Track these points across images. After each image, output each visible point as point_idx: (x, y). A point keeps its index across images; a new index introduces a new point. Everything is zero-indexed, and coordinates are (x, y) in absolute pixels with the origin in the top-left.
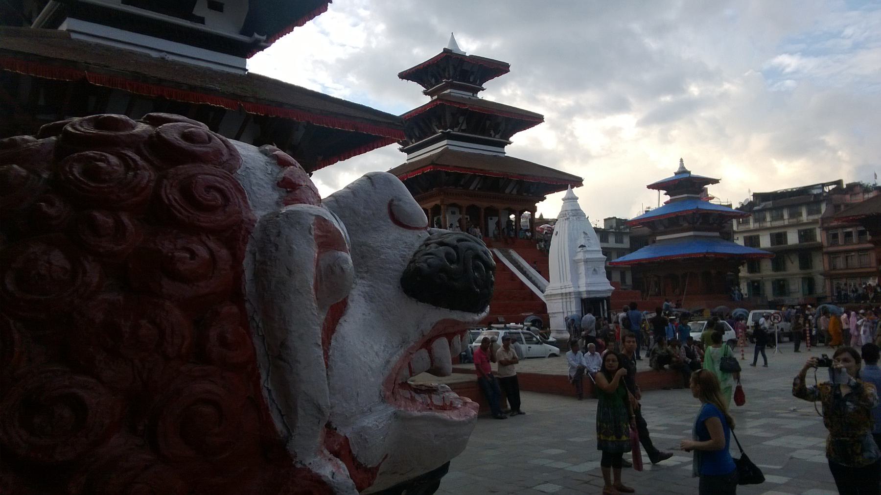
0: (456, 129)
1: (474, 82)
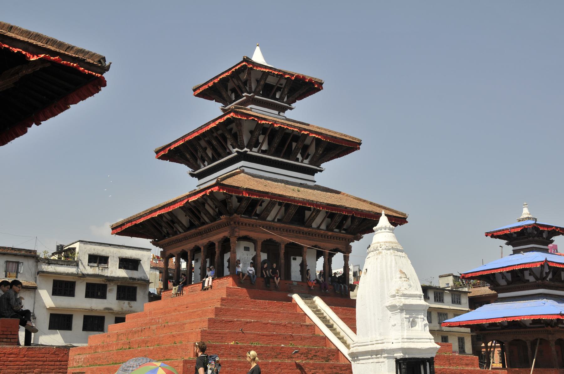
0: (254, 149)
1: (281, 99)
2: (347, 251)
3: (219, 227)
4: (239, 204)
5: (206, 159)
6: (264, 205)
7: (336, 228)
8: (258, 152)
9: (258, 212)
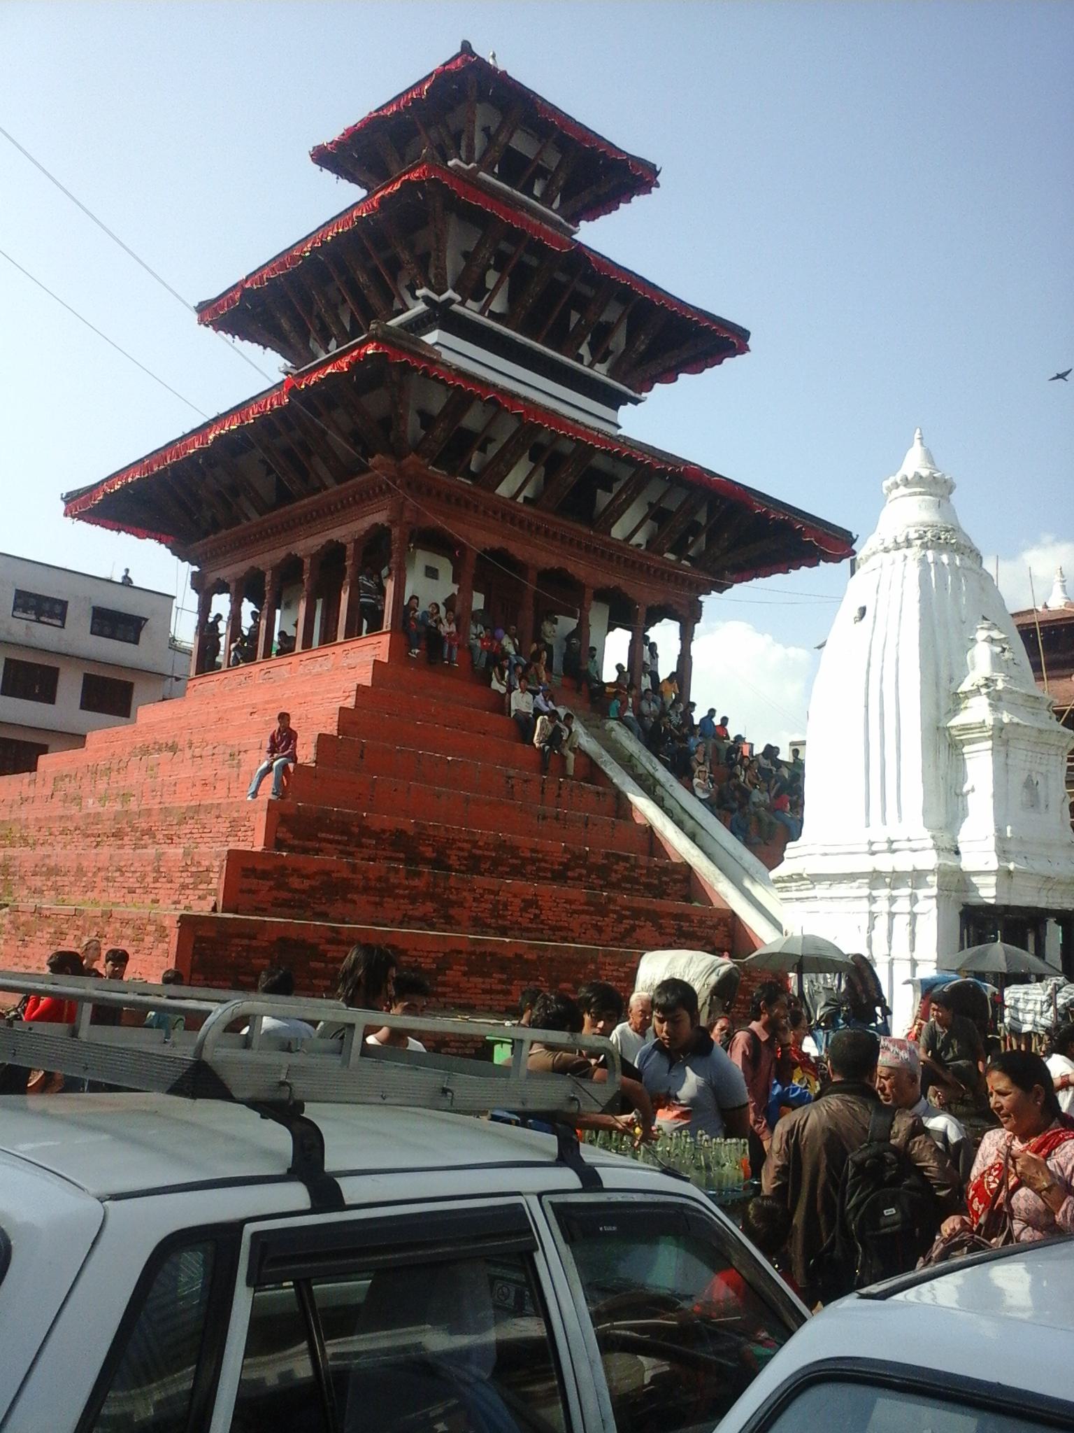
0: (470, 303)
1: (546, 199)
2: (688, 619)
3: (362, 499)
4: (423, 432)
5: (334, 330)
6: (493, 449)
7: (671, 551)
8: (481, 313)
9: (473, 468)
